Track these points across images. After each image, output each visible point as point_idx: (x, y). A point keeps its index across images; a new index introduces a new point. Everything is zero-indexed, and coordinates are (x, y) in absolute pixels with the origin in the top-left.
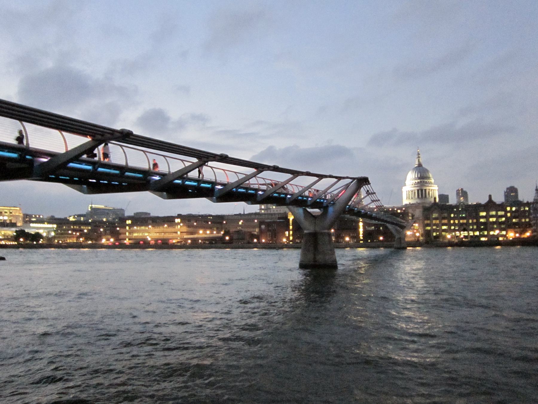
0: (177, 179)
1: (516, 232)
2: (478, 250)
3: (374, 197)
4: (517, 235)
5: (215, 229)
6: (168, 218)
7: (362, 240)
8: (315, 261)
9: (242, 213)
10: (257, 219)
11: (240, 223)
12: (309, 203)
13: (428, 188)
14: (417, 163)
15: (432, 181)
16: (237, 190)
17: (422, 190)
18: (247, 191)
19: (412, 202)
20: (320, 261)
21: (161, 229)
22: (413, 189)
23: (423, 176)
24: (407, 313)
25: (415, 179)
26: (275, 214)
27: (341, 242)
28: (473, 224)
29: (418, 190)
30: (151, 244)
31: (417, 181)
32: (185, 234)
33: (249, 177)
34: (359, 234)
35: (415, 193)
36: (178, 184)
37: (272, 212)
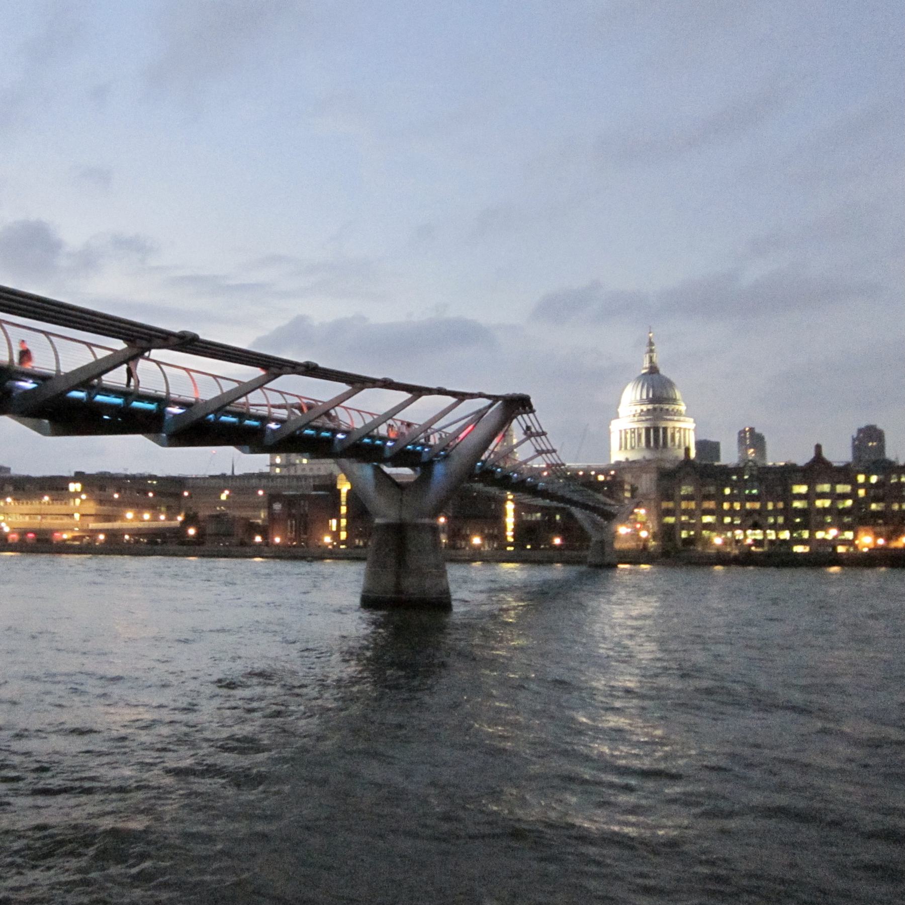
0: (76, 388)
1: (877, 535)
2: (787, 574)
3: (542, 443)
4: (881, 541)
5: (163, 509)
6: (52, 479)
7: (511, 545)
8: (399, 591)
9: (229, 473)
10: (263, 488)
11: (223, 497)
12: (388, 454)
13: (670, 425)
14: (646, 364)
15: (682, 407)
16: (217, 418)
17: (656, 430)
18: (241, 422)
19: (633, 456)
20: (411, 590)
21: (33, 506)
22: (635, 425)
23: (660, 396)
24: (613, 721)
25: (642, 402)
26: (306, 477)
27: (460, 548)
28: (775, 512)
29: (648, 430)
30: (10, 541)
31: (645, 408)
32: (92, 518)
33: (246, 389)
34: (504, 529)
35: (639, 435)
36: (78, 401)
37: (299, 473)
